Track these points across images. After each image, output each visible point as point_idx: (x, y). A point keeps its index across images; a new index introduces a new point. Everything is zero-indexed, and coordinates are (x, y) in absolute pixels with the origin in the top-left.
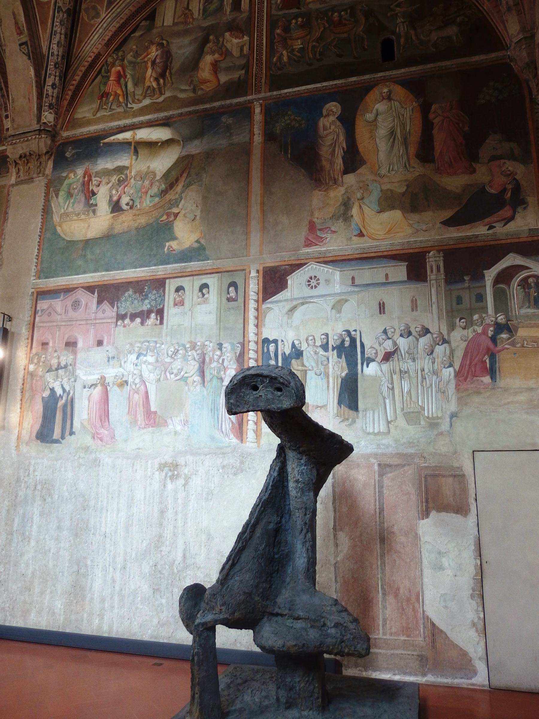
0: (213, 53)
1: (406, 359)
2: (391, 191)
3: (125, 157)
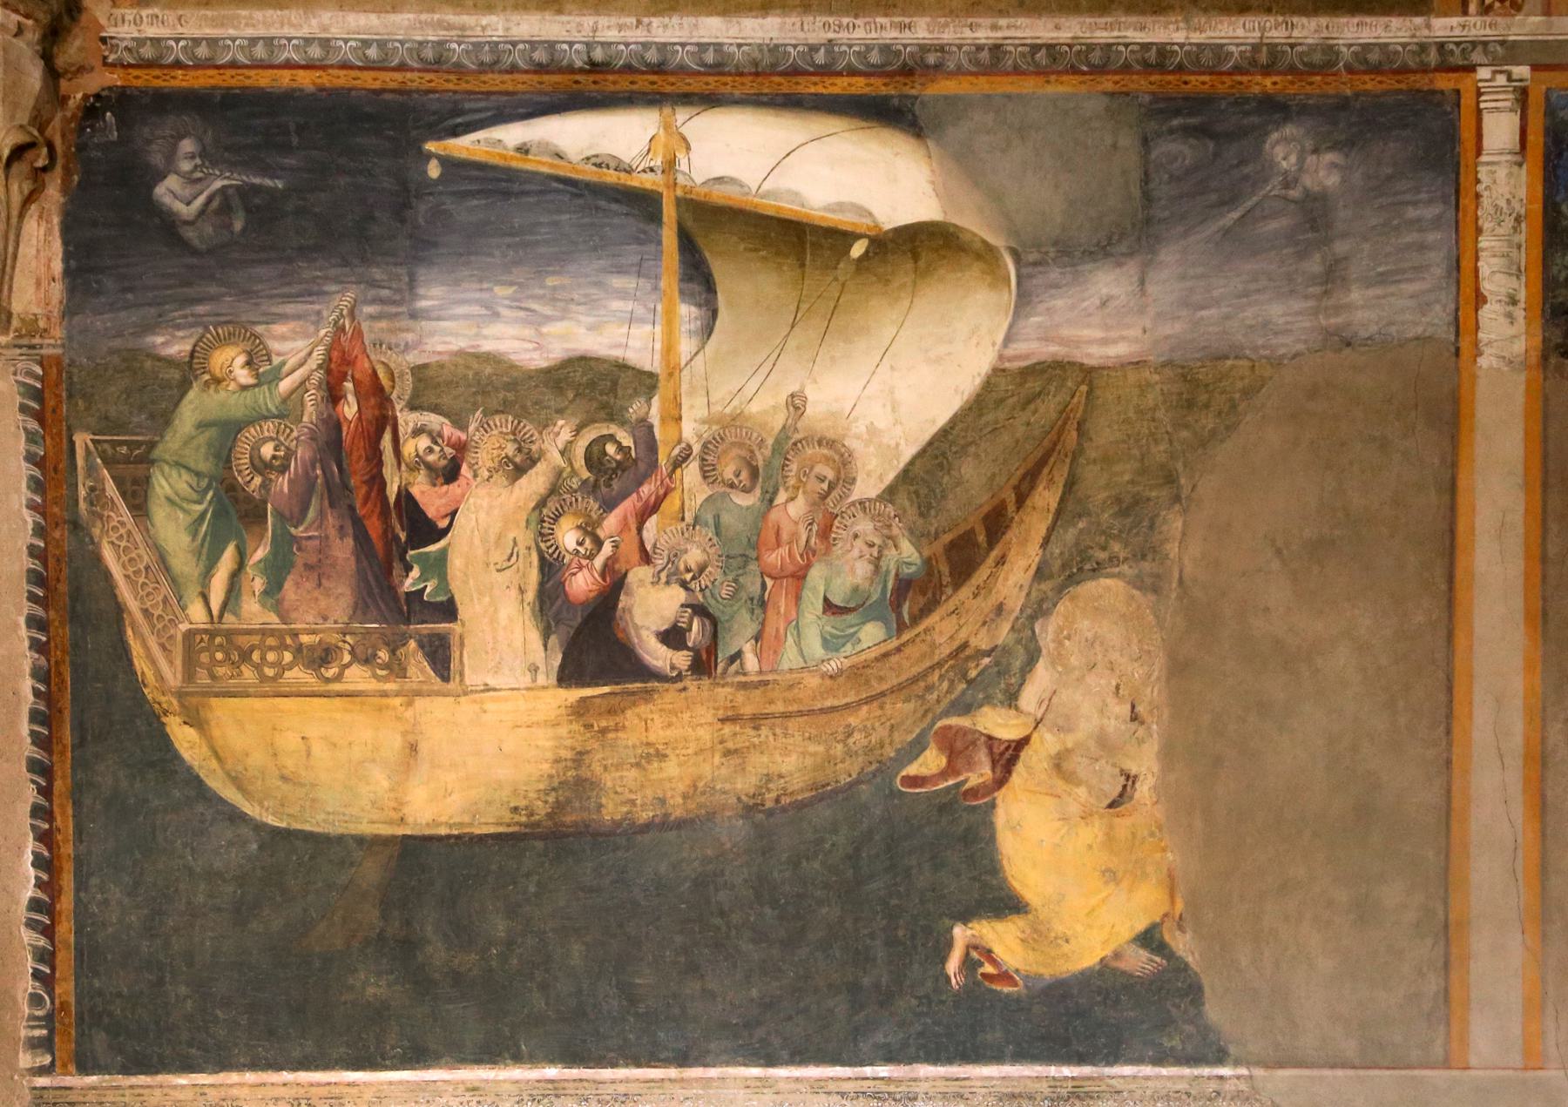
3: (623, 295)
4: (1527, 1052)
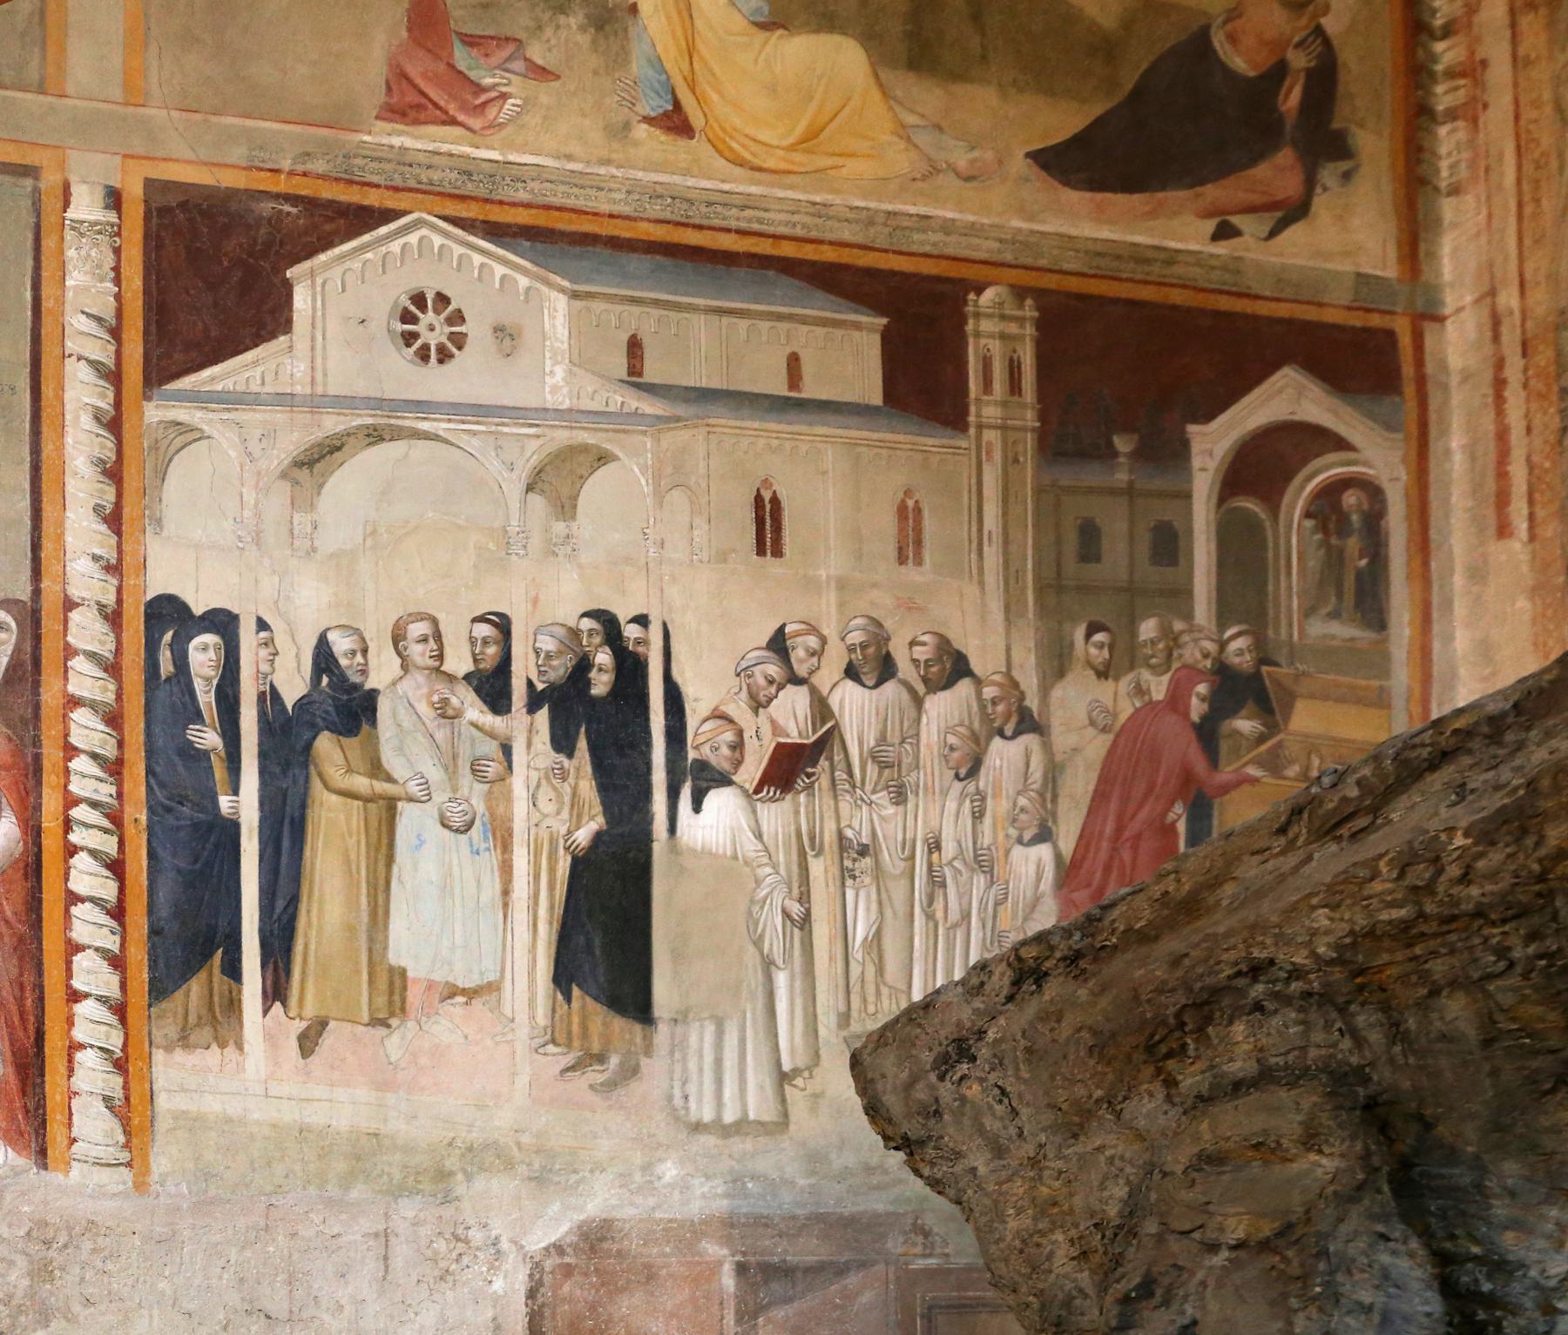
1: (868, 788)
4: (128, 86)
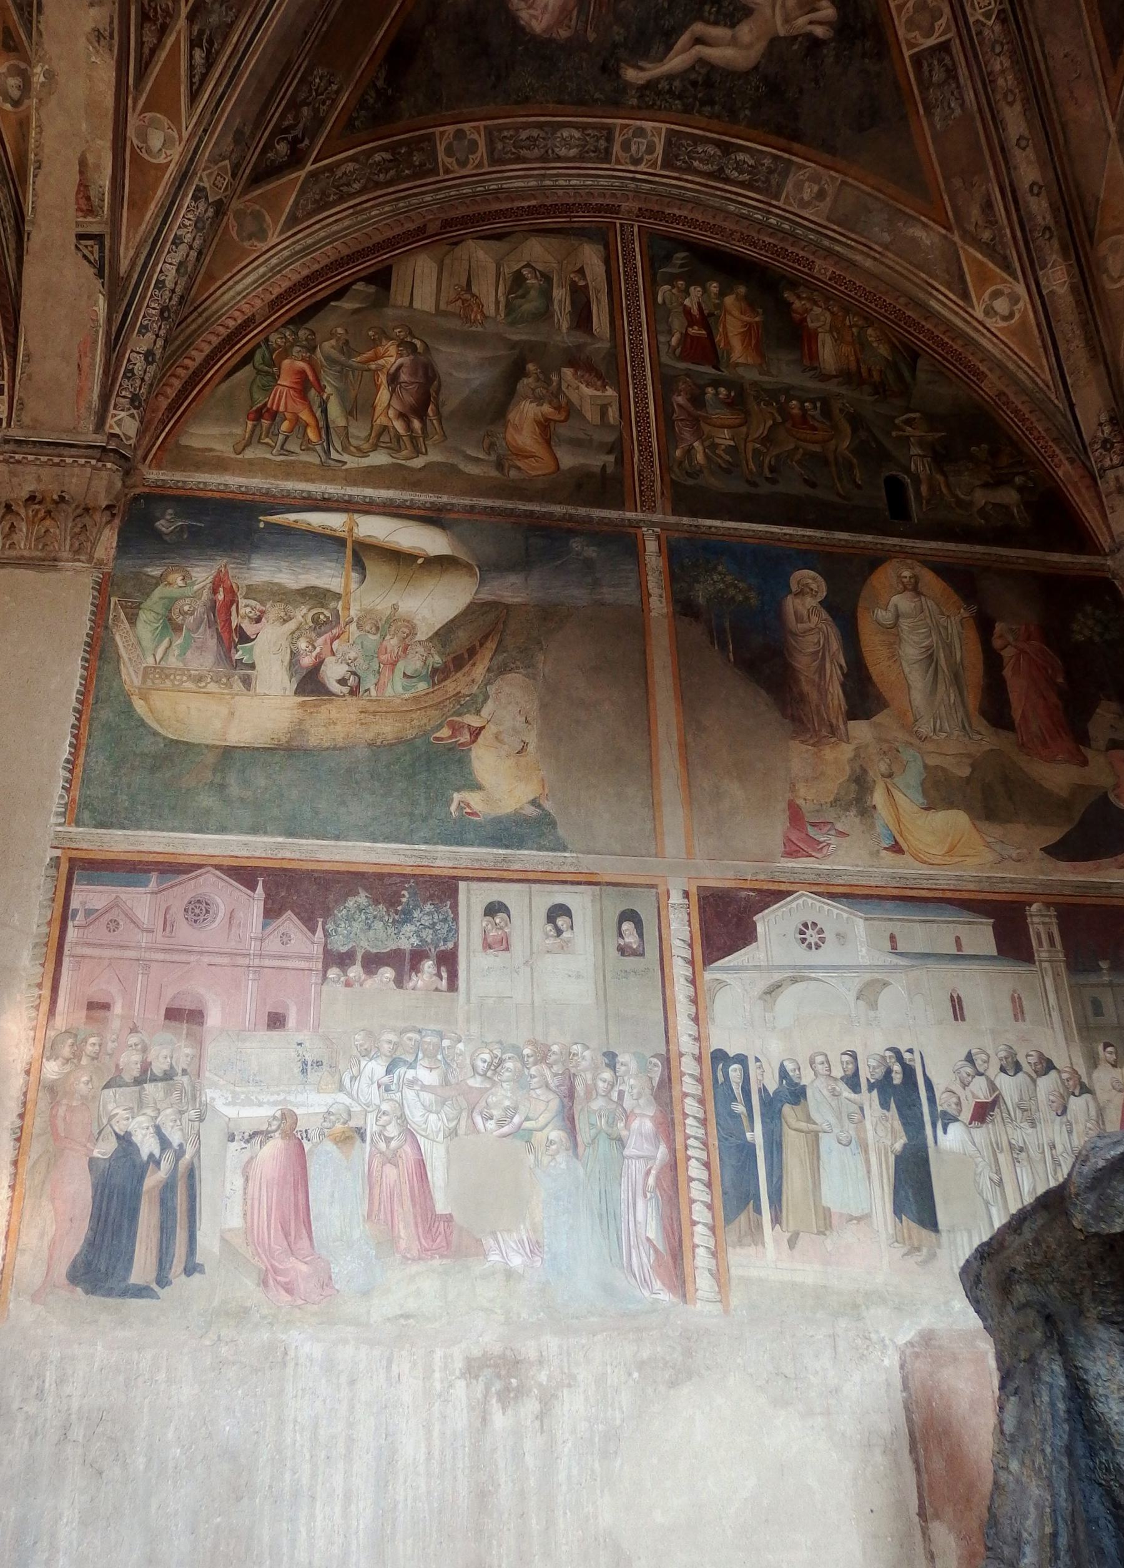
0: (539, 400)
2: (943, 770)
3: (330, 568)
